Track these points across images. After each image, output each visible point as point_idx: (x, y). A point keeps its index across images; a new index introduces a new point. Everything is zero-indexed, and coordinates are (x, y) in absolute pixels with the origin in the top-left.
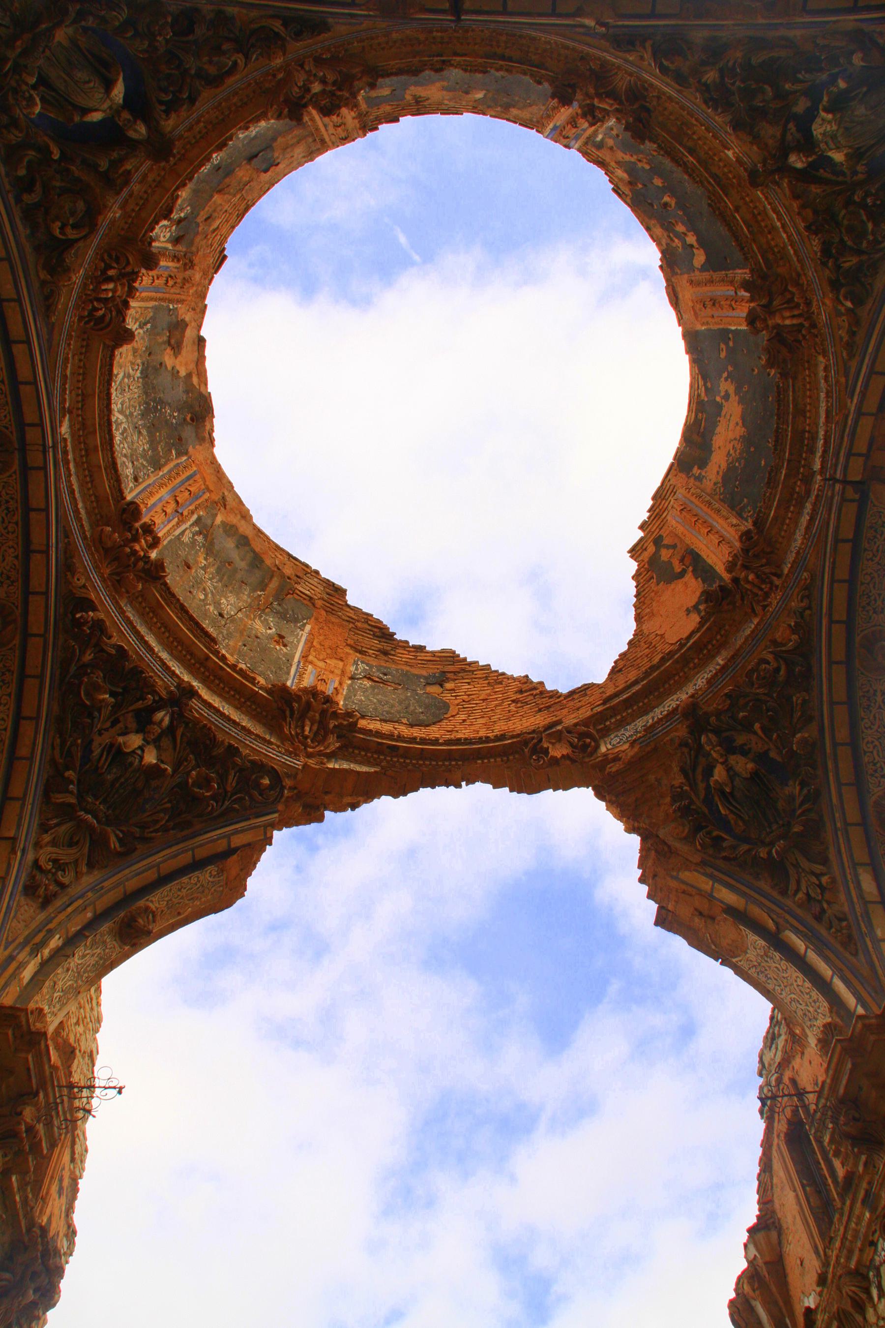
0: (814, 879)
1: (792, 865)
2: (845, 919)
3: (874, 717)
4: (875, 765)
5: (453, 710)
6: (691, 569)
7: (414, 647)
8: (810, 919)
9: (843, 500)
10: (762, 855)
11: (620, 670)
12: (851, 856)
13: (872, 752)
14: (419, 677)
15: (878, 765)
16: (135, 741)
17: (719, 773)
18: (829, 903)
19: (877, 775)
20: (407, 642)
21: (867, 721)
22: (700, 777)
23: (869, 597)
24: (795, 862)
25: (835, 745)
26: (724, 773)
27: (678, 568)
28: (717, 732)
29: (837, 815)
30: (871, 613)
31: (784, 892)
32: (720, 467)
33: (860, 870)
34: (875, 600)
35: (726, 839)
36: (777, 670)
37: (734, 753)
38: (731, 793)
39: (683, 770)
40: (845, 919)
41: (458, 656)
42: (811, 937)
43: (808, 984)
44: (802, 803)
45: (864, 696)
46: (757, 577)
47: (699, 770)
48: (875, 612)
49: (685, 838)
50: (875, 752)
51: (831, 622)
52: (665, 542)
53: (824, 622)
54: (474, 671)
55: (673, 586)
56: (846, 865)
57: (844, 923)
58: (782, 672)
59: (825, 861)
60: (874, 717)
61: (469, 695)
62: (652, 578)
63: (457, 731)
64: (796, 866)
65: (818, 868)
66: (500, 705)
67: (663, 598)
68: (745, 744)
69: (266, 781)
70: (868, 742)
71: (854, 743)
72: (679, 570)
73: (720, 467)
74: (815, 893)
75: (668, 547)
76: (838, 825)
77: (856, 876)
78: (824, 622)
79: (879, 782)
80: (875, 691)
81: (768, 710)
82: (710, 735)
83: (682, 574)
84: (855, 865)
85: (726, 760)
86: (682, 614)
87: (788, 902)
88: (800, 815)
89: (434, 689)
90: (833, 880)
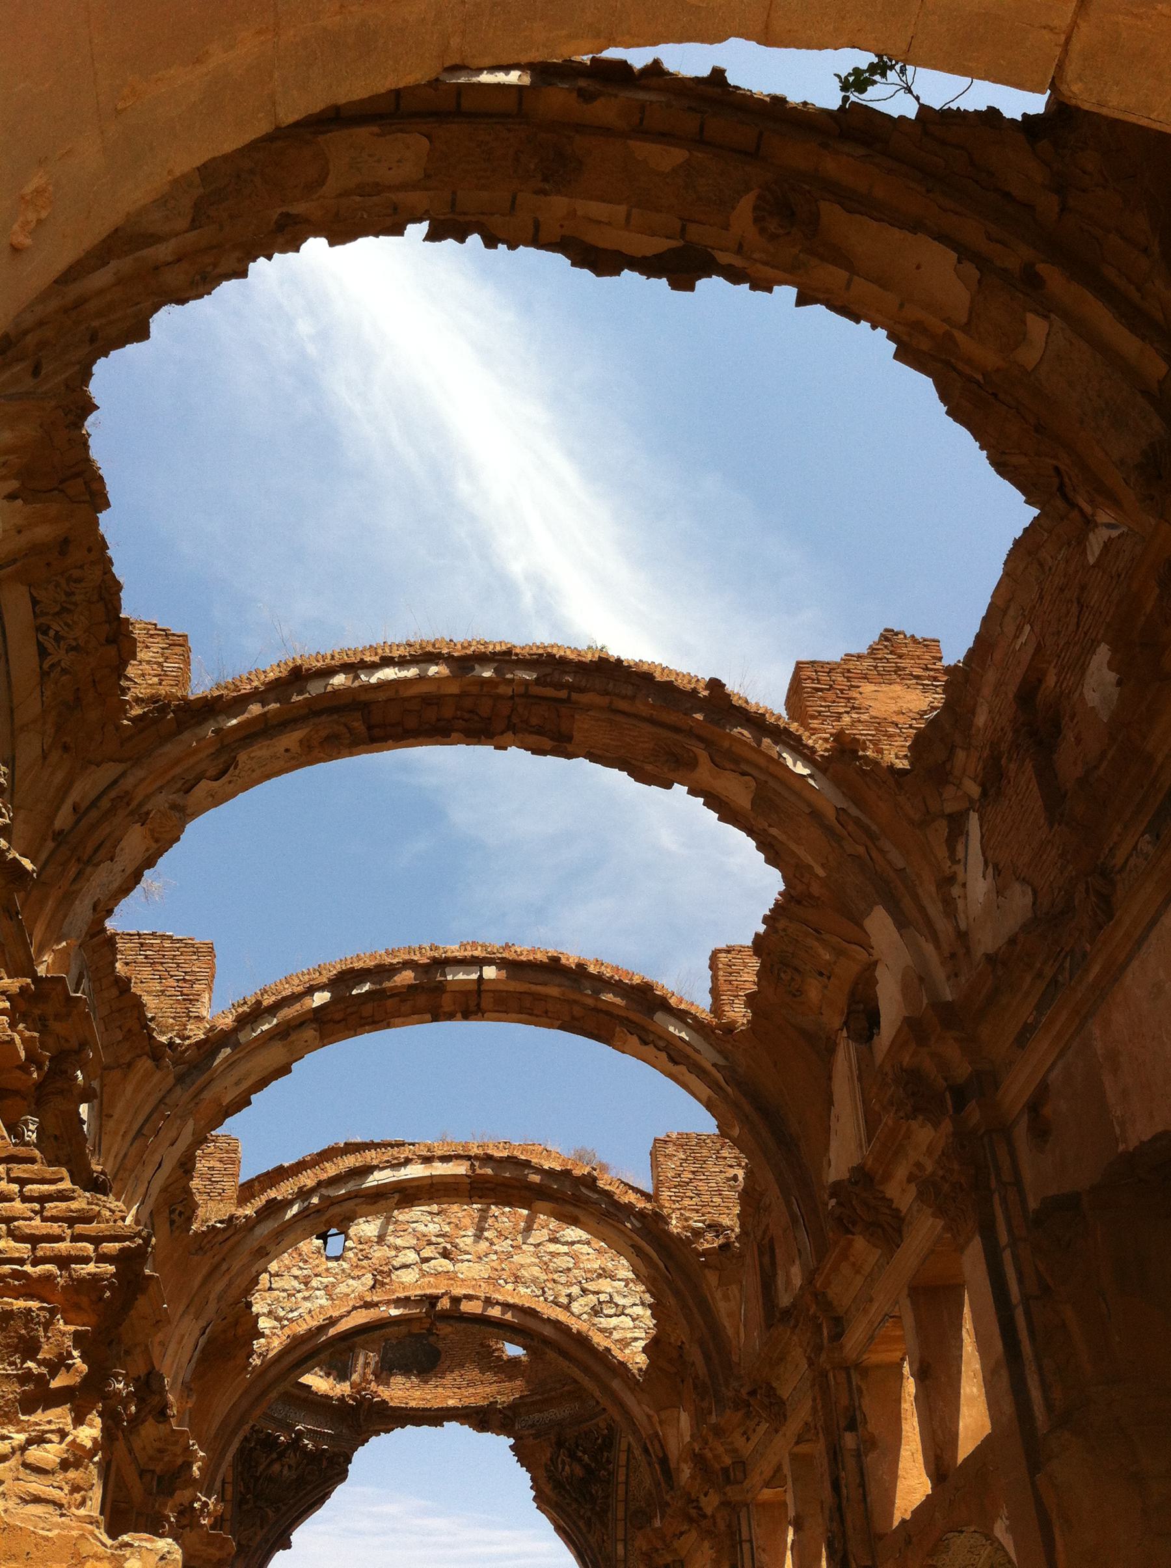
16: (276, 1467)
58: (600, 1441)
69: (342, 1459)
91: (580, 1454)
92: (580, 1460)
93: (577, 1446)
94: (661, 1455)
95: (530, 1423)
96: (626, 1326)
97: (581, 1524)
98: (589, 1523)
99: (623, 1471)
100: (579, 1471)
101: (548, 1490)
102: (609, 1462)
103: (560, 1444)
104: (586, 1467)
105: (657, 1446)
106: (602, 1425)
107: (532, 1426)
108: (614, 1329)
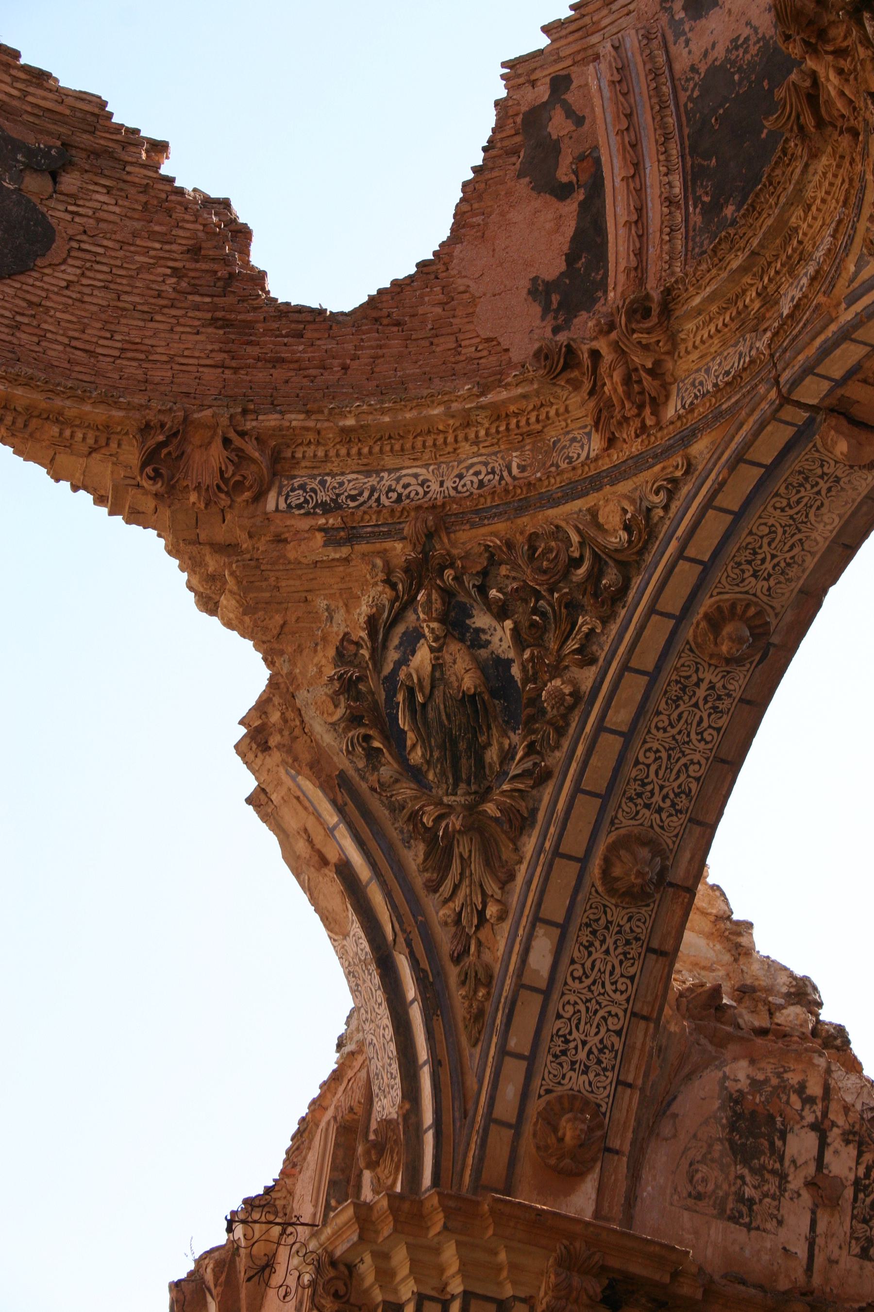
0: (478, 900)
1: (461, 856)
2: (488, 985)
3: (680, 716)
4: (644, 785)
5: (59, 248)
6: (580, 195)
7: (27, 69)
9: (775, 416)
13: (648, 766)
14: (18, 146)
19: (639, 801)
20: (16, 54)
21: (665, 718)
22: (396, 641)
23: (755, 553)
24: (466, 856)
25: (600, 728)
27: (564, 174)
28: (447, 594)
29: (552, 830)
30: (747, 575)
32: (713, 46)
33: (540, 931)
34: (763, 561)
36: (577, 563)
37: (462, 640)
41: (110, 115)
43: (392, 1047)
45: (677, 682)
47: (400, 629)
48: (755, 575)
49: (333, 724)
50: (653, 768)
51: (680, 555)
54: (127, 163)
55: (537, 204)
56: (526, 912)
58: (582, 571)
60: (680, 716)
61: (99, 220)
62: (515, 152)
63: (48, 309)
64: (465, 862)
65: (492, 887)
66: (149, 268)
67: (514, 216)
68: (483, 631)
70: (650, 750)
72: (564, 179)
73: (713, 46)
75: (570, 113)
76: (547, 845)
77: (530, 937)
79: (637, 813)
80: (699, 681)
81: (535, 611)
82: (435, 596)
83: (563, 192)
84: (537, 919)
85: (440, 649)
86: (524, 284)
89: (35, 184)
91: (482, 620)
92: (475, 641)
93: (483, 590)
95: (323, 496)
97: (414, 857)
98: (440, 854)
100: (464, 675)
101: (323, 721)
103: (420, 571)
106: (611, 517)
107: (326, 508)
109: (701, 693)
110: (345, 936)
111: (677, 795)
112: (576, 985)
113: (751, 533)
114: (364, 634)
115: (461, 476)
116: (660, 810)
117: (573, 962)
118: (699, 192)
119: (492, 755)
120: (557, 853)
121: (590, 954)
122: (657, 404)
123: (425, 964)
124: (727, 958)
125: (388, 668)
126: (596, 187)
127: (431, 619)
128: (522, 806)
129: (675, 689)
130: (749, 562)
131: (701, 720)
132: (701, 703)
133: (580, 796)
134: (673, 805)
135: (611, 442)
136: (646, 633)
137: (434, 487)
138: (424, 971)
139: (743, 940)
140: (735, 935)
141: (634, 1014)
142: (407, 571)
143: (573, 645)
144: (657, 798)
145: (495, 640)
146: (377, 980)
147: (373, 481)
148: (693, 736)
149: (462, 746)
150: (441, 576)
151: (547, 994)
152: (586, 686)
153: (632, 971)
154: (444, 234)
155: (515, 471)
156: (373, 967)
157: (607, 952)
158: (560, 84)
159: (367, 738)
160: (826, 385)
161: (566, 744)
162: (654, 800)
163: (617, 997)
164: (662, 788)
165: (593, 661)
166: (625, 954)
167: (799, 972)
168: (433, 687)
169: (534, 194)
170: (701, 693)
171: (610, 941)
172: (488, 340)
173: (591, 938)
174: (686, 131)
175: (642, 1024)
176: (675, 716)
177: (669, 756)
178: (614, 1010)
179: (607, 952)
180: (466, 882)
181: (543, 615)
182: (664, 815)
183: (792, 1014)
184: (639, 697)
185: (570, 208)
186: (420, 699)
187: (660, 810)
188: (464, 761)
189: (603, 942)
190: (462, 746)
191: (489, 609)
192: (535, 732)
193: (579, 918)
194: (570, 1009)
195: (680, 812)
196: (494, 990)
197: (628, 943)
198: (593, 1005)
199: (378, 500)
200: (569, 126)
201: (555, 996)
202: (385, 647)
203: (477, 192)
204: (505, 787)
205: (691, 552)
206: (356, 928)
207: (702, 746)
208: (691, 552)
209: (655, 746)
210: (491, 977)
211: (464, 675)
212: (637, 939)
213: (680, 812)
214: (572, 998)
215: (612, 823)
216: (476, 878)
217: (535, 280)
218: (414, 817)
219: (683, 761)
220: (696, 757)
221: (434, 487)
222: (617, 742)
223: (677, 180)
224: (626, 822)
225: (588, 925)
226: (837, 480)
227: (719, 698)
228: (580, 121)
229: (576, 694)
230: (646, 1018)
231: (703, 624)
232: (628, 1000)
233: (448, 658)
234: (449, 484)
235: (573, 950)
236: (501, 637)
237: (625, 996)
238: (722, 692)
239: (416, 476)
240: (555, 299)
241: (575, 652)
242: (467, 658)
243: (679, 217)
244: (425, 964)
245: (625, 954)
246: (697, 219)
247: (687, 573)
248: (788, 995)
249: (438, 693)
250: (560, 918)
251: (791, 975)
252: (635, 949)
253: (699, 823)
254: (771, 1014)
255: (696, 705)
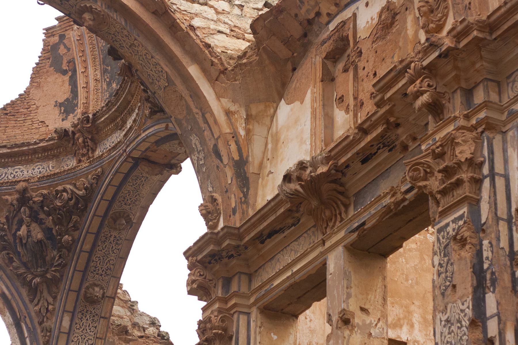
0: (46, 304)
2: (50, 332)
3: (106, 246)
4: (96, 268)
6: (70, 73)
8: (36, 321)
10: (28, 279)
11: (6, 114)
12: (65, 306)
15: (97, 268)
17: (23, 231)
18: (47, 318)
22: (16, 222)
23: (124, 198)
25: (81, 251)
26: (26, 232)
28: (31, 208)
31: (31, 301)
33: (65, 314)
34: (127, 200)
35: (15, 261)
37: (36, 222)
38: (25, 244)
39: (7, 218)
40: (50, 332)
42: (32, 333)
44: (56, 266)
46: (84, 142)
48: (125, 204)
50: (98, 262)
51: (102, 198)
52: (65, 41)
53: (99, 196)
55: (57, 76)
57: (48, 334)
58: (72, 202)
59: (55, 298)
60: (106, 246)
62: (49, 58)
64: (42, 293)
65: (51, 300)
67: (49, 79)
68: (43, 219)
71: (91, 253)
72: (65, 68)
74: (44, 311)
75: (65, 46)
76: (67, 287)
78: (99, 196)
81: (59, 214)
82: (27, 209)
83: (64, 73)
84: (64, 311)
85: (29, 226)
87: (30, 306)
88: (52, 271)
90: (54, 309)
91: (42, 216)
93: (42, 207)
94: (236, 157)
96: (210, 17)
99: (91, 238)
100: (38, 234)
102: (76, 228)
104: (48, 231)
105: (233, 147)
108: (196, 15)
109: (112, 239)
110: (5, 316)
111: (107, 270)
112: (78, 331)
113: (122, 193)
114: (5, 221)
115: (34, 169)
116: (101, 275)
117: (76, 324)
118: (106, 77)
119: (48, 258)
120: (69, 290)
121: (82, 321)
122: (94, 151)
123: (30, 326)
124: (129, 314)
125: (13, 232)
126: (74, 71)
127: (27, 217)
128: (58, 275)
129: (103, 239)
130: (123, 201)
131: (113, 247)
132: (112, 242)
133: (76, 272)
134: (106, 273)
135: (80, 161)
136: (93, 222)
137: (25, 173)
138: (29, 328)
139: (135, 308)
140: (131, 306)
141: (97, 338)
142: (17, 201)
143: (71, 225)
144: (100, 271)
145: (47, 222)
146: (15, 330)
147: (6, 170)
148: (110, 252)
149: (38, 256)
150: (28, 203)
151: (69, 334)
152: (76, 237)
153: (95, 325)
154: (28, 84)
155: (51, 168)
156: (14, 326)
157: (87, 320)
158: (62, 37)
159: (8, 254)
160: (140, 153)
161: (71, 255)
162: (99, 272)
163: (91, 333)
164: (102, 268)
165: (78, 229)
166: (93, 320)
167: (153, 315)
168: (28, 238)
169: (55, 73)
170: (112, 239)
171: (88, 316)
172: (42, 122)
173: (82, 316)
174: (101, 56)
175: (100, 341)
176: (104, 246)
177: (103, 259)
178: (90, 338)
179: (87, 320)
180: (42, 299)
181: (61, 215)
182: (103, 276)
183: (151, 330)
184: (92, 241)
185: (67, 78)
186: (24, 242)
187: (101, 275)
188: (39, 261)
189: (86, 317)
190: (38, 256)
191: (44, 213)
192: (61, 251)
193: (78, 310)
194: (76, 339)
195: (108, 275)
196: (52, 334)
197: (94, 316)
198: (83, 337)
199: (7, 177)
200: (65, 51)
201: (71, 334)
202: (12, 224)
203: (38, 72)
204: (53, 269)
205: (105, 198)
206: (8, 314)
207: (113, 255)
208: (105, 198)
209: (99, 256)
210: (51, 329)
211: (38, 234)
212: (97, 315)
213: (108, 275)
214: (77, 335)
215: (86, 280)
216: (45, 297)
217: (56, 102)
218: (25, 279)
219: (108, 259)
220: (112, 258)
221: (25, 173)
222: (86, 255)
223: (98, 73)
224: (91, 279)
225: (80, 312)
226: (147, 178)
227: (118, 240)
228: (69, 49)
229: (73, 240)
230: (101, 339)
231: (111, 220)
232: (95, 334)
233: (32, 229)
234: (30, 172)
235: (76, 320)
236: (49, 221)
237: (94, 333)
238: (119, 238)
239: (20, 169)
240: (63, 109)
241: (72, 227)
242: (38, 228)
243: (100, 85)
244: (30, 326)
245: (93, 320)
246: (105, 86)
247: (104, 205)
248: (150, 324)
249: (29, 240)
250: (72, 310)
251: (150, 318)
252: (96, 318)
253: (114, 277)
254: (144, 331)
255: (111, 243)
